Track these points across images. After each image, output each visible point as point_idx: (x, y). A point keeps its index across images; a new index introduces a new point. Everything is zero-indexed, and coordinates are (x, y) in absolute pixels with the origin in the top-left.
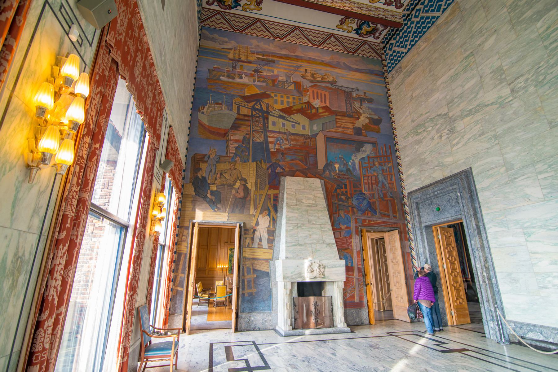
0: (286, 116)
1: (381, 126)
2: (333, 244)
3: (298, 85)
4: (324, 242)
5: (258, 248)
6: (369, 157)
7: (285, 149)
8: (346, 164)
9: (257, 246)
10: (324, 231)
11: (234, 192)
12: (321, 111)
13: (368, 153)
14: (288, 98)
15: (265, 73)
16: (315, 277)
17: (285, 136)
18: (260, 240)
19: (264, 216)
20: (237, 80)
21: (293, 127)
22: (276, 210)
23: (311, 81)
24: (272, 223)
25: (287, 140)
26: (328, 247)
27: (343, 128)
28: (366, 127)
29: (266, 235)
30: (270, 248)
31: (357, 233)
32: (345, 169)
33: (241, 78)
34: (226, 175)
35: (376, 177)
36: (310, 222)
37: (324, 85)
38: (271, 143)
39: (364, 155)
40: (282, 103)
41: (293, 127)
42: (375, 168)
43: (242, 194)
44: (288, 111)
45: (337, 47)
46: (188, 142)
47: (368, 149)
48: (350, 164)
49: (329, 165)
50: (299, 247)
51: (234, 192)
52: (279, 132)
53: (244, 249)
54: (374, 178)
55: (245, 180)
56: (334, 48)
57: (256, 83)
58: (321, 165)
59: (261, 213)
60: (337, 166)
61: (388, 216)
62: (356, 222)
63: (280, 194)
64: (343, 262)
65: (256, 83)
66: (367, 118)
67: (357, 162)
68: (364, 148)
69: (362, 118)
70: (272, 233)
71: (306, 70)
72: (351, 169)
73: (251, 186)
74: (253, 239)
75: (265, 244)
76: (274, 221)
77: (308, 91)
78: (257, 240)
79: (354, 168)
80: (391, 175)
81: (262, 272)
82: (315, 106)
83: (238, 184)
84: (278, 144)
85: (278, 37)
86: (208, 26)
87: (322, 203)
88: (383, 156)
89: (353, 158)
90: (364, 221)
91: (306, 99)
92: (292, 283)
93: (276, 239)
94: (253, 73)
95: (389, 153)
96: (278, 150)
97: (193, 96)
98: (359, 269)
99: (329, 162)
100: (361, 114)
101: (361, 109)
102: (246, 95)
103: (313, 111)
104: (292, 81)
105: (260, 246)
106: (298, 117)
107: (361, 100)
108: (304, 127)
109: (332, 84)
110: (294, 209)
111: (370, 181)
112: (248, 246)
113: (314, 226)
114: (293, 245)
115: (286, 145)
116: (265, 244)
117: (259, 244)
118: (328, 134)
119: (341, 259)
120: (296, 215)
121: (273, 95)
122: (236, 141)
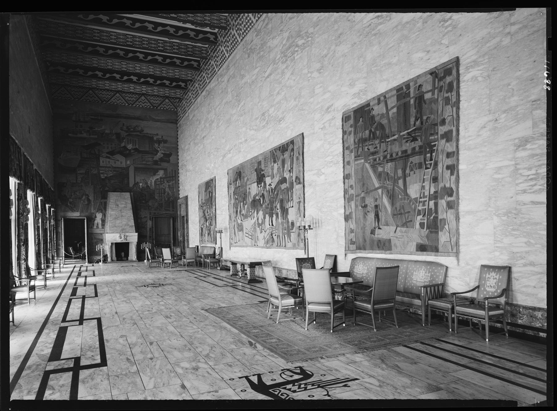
1: (171, 158)
3: (118, 135)
6: (161, 178)
7: (110, 176)
8: (147, 183)
11: (82, 202)
12: (132, 151)
13: (161, 176)
14: (112, 144)
15: (96, 129)
17: (110, 169)
18: (98, 224)
20: (79, 135)
21: (115, 163)
23: (127, 132)
25: (111, 171)
27: (147, 161)
28: (161, 160)
29: (100, 222)
30: (103, 228)
31: (150, 219)
33: (82, 133)
34: (77, 193)
35: (164, 190)
37: (135, 133)
38: (102, 173)
39: (158, 177)
40: (108, 148)
41: (115, 163)
42: (164, 184)
43: (86, 203)
44: (112, 153)
45: (145, 104)
47: (161, 173)
49: (136, 184)
50: (115, 228)
51: (82, 202)
52: (106, 167)
53: (89, 229)
54: (163, 190)
55: (88, 195)
56: (143, 105)
57: (92, 136)
58: (131, 185)
60: (141, 184)
61: (169, 210)
62: (150, 214)
65: (92, 136)
67: (153, 181)
70: (103, 221)
73: (91, 198)
75: (100, 226)
76: (104, 215)
77: (124, 138)
78: (95, 225)
79: (151, 185)
80: (173, 188)
81: (99, 239)
83: (84, 197)
87: (130, 206)
88: (170, 177)
89: (151, 179)
90: (155, 213)
91: (123, 145)
95: (174, 175)
96: (106, 177)
100: (158, 151)
103: (127, 152)
105: (98, 227)
106: (118, 157)
107: (159, 142)
108: (121, 163)
109: (140, 133)
115: (110, 174)
116: (100, 226)
118: (136, 166)
121: (102, 144)
122: (81, 174)
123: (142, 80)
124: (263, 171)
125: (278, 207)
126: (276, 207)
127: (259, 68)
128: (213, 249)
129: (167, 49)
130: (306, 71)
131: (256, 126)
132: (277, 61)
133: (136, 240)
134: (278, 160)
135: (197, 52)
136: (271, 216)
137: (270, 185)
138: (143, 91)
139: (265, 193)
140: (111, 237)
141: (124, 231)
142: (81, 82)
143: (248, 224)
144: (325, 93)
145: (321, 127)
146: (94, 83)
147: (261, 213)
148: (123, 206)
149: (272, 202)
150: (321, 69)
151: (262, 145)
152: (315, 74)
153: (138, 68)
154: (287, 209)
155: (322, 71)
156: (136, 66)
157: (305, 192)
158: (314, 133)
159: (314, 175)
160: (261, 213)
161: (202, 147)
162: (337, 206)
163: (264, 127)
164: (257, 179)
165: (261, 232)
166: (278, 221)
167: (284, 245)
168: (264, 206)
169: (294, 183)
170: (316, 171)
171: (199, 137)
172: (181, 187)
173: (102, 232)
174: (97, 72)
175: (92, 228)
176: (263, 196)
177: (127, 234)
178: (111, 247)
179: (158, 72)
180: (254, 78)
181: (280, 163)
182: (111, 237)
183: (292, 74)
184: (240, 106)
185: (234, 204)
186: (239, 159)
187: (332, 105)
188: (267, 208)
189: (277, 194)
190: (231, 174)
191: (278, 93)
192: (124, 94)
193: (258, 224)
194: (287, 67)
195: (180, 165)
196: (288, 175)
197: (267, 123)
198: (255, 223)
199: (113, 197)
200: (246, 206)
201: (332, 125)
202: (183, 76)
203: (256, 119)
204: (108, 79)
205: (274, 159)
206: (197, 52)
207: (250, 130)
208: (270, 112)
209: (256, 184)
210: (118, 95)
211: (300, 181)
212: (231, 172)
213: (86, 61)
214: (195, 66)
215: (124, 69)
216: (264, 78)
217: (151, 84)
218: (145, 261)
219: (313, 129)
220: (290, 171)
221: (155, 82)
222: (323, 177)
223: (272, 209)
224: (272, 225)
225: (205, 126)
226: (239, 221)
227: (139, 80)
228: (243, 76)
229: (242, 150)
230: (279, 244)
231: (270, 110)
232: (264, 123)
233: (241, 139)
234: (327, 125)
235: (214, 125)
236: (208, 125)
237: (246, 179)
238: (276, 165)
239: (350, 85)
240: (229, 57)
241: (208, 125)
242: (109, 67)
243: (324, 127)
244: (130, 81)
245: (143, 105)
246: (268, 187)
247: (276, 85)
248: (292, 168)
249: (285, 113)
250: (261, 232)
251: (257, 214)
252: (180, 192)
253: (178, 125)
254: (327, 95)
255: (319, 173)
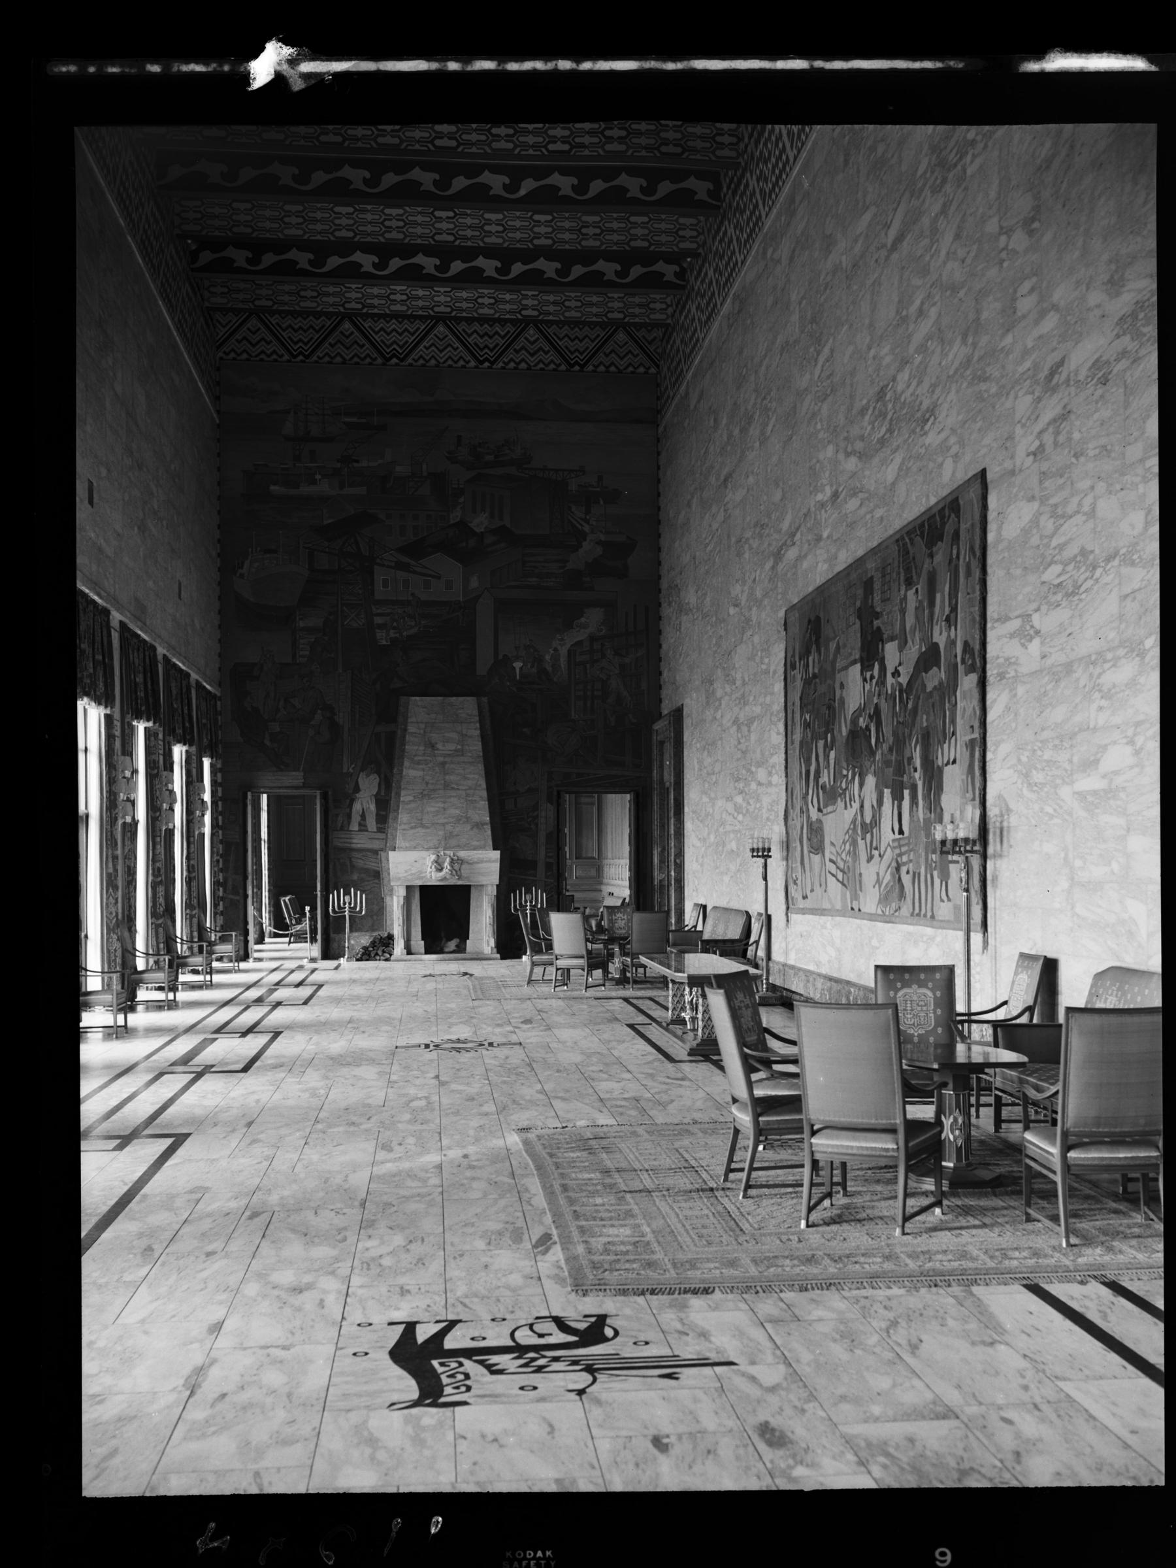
0: (413, 562)
2: (483, 824)
4: (468, 819)
5: (360, 830)
6: (592, 639)
9: (356, 828)
10: (472, 802)
16: (445, 879)
18: (363, 816)
19: (368, 776)
22: (391, 766)
24: (383, 786)
26: (475, 830)
29: (373, 807)
30: (380, 830)
32: (534, 670)
36: (447, 786)
39: (582, 635)
46: (220, 641)
47: (593, 619)
48: (548, 657)
56: (532, 360)
58: (482, 668)
59: (362, 770)
60: (518, 665)
63: (399, 732)
64: (497, 854)
66: (599, 543)
67: (563, 651)
68: (583, 620)
69: (586, 545)
71: (459, 437)
72: (549, 669)
74: (349, 816)
78: (356, 819)
82: (477, 530)
83: (318, 716)
84: (394, 628)
85: (394, 356)
86: (233, 355)
87: (476, 747)
91: (456, 516)
92: (408, 888)
93: (391, 815)
94: (339, 465)
97: (219, 541)
98: (548, 866)
99: (500, 657)
101: (587, 522)
102: (326, 522)
104: (425, 474)
105: (363, 827)
110: (418, 763)
111: (589, 693)
112: (342, 829)
113: (453, 793)
114: (412, 828)
116: (371, 823)
117: (360, 824)
119: (495, 849)
120: (420, 773)
123: (517, 268)
124: (877, 615)
125: (918, 762)
126: (910, 759)
127: (873, 209)
128: (741, 921)
129: (582, 146)
130: (992, 226)
131: (862, 438)
132: (920, 185)
133: (495, 879)
134: (919, 576)
135: (699, 144)
136: (898, 797)
137: (896, 673)
138: (526, 307)
139: (884, 707)
140: (410, 864)
141: (453, 842)
142: (309, 293)
143: (838, 822)
144: (1042, 314)
145: (1032, 449)
146: (354, 294)
147: (871, 781)
148: (452, 746)
149: (900, 743)
150: (1033, 220)
151: (879, 513)
152: (1019, 240)
153: (494, 228)
154: (940, 771)
155: (1036, 225)
156: (489, 222)
157: (988, 703)
158: (1012, 473)
159: (1012, 636)
160: (871, 781)
161: (721, 516)
162: (1071, 761)
163: (882, 442)
164: (862, 649)
165: (870, 858)
166: (913, 813)
167: (929, 914)
168: (878, 757)
169: (961, 668)
170: (1015, 624)
171: (713, 480)
172: (665, 674)
173: (376, 845)
174: (358, 257)
175: (345, 828)
176: (876, 716)
177: (462, 854)
178: (408, 900)
179: (567, 236)
180: (858, 248)
181: (921, 586)
182: (410, 864)
183: (957, 236)
184: (821, 360)
185: (801, 743)
186: (818, 566)
187: (1061, 363)
188: (887, 763)
189: (915, 710)
190: (795, 630)
191: (921, 312)
192: (463, 326)
193: (863, 824)
194: (944, 211)
195: (664, 584)
196: (945, 634)
197: (890, 431)
198: (854, 821)
199: (420, 711)
200: (832, 754)
201: (1061, 439)
202: (664, 238)
203: (863, 412)
204: (400, 275)
205: (908, 570)
206: (699, 144)
207: (847, 455)
208: (900, 387)
209: (858, 666)
210: (441, 328)
211: (977, 659)
212: (795, 617)
213: (315, 221)
214: (702, 195)
215: (445, 237)
216: (884, 253)
217: (551, 282)
218: (524, 958)
219: (1012, 457)
220: (948, 620)
221: (563, 272)
222: (1035, 646)
223: (900, 770)
224: (901, 832)
225: (730, 436)
226: (814, 814)
227: (504, 270)
228: (829, 243)
229: (825, 535)
230: (917, 911)
231: (899, 377)
232: (884, 430)
233: (823, 491)
234: (1048, 438)
235: (754, 431)
236: (736, 432)
237: (833, 646)
238: (911, 593)
239: (1111, 281)
240: (795, 158)
241: (736, 432)
242: (394, 235)
243: (1042, 447)
244: (473, 277)
245: (532, 360)
246: (890, 680)
247: (917, 281)
248: (954, 609)
249: (938, 390)
250: (870, 858)
251: (861, 785)
252: (664, 693)
253: (661, 429)
254: (1050, 323)
255: (1026, 634)
